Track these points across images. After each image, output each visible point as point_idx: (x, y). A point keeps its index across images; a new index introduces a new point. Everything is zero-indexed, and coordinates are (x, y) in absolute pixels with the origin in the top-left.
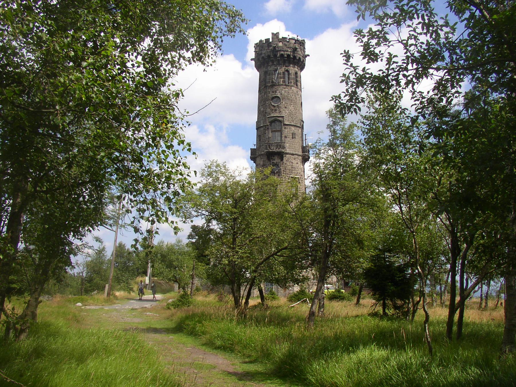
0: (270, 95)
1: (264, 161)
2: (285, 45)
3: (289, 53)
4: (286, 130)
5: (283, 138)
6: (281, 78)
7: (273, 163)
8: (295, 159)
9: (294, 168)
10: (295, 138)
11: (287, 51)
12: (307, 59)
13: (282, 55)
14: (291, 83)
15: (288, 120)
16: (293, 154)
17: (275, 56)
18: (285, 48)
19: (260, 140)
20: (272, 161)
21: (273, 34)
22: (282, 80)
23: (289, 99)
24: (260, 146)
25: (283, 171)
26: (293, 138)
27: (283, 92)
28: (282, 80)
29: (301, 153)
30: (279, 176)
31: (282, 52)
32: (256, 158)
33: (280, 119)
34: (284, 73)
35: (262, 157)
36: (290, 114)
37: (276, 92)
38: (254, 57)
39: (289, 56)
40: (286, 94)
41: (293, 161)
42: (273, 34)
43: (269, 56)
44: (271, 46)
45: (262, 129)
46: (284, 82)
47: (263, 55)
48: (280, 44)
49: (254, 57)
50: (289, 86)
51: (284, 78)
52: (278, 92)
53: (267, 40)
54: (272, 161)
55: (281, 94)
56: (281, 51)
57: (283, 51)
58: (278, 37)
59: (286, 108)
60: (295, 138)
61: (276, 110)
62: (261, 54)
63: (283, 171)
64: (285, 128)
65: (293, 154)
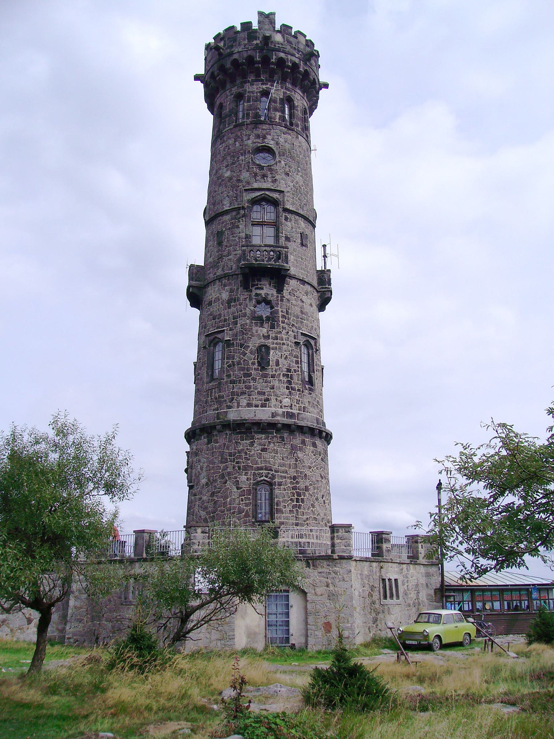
0: (250, 142)
1: (231, 291)
2: (289, 42)
3: (297, 61)
4: (289, 224)
5: (282, 241)
6: (276, 110)
7: (257, 295)
8: (307, 293)
9: (306, 314)
10: (306, 246)
11: (293, 55)
12: (323, 93)
13: (281, 62)
14: (297, 126)
15: (293, 204)
16: (303, 282)
17: (266, 60)
18: (288, 48)
19: (220, 244)
20: (254, 292)
21: (261, 14)
22: (278, 114)
23: (292, 158)
24: (221, 258)
25: (283, 316)
26: (302, 245)
27: (281, 140)
28: (278, 114)
29: (315, 284)
30: (273, 327)
31: (282, 55)
32: (206, 286)
33: (275, 195)
34: (282, 100)
35: (225, 281)
36: (297, 190)
37: (264, 137)
38: (202, 71)
39: (295, 66)
40: (287, 146)
41: (304, 298)
42: (261, 14)
43: (250, 60)
44: (256, 38)
45: (227, 218)
46: (283, 118)
47: (236, 56)
48: (278, 38)
49: (202, 71)
50: (293, 130)
51: (283, 112)
52: (269, 137)
53: (246, 26)
54: (254, 292)
55: (277, 144)
56: (279, 50)
57: (284, 52)
58: (272, 23)
59: (287, 174)
60: (306, 246)
61: (264, 176)
62: (232, 54)
63: (283, 316)
64: (286, 219)
65: (303, 282)
